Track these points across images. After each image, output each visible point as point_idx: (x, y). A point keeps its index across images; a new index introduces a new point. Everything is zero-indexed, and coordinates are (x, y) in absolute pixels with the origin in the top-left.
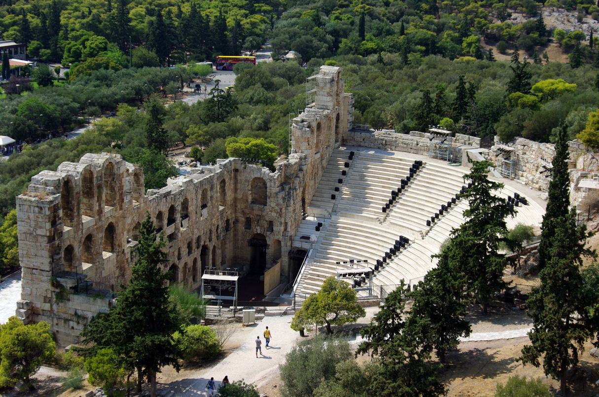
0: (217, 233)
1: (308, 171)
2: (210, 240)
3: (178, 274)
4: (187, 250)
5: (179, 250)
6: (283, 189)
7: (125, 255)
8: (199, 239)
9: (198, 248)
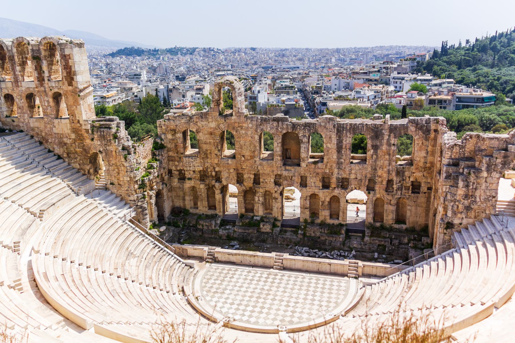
4: (321, 184)
6: (455, 164)
7: (81, 125)
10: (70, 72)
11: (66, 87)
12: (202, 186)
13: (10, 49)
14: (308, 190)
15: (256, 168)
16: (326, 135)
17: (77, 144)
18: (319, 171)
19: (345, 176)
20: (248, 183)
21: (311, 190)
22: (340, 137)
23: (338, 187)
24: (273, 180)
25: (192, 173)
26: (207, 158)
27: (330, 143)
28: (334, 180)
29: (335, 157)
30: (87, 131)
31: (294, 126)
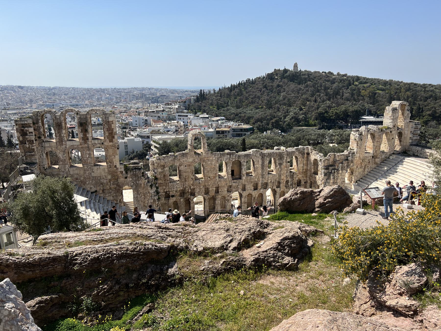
1: (355, 162)
2: (278, 187)
4: (253, 188)
7: (117, 169)
10: (112, 132)
11: (107, 143)
12: (182, 200)
13: (58, 117)
16: (256, 160)
17: (112, 182)
18: (252, 180)
19: (265, 181)
20: (212, 193)
22: (263, 160)
23: (262, 188)
24: (226, 189)
25: (174, 192)
26: (186, 181)
28: (260, 185)
30: (122, 172)
31: (239, 156)
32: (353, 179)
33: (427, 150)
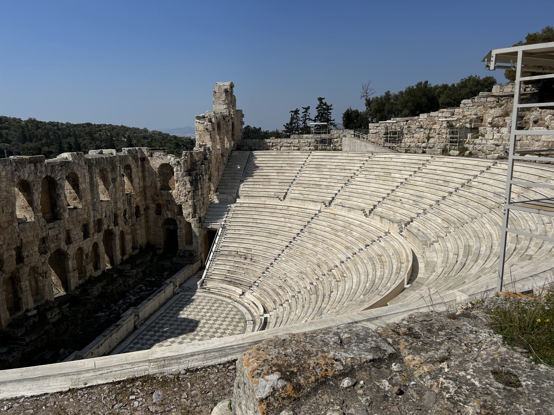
0: (125, 218)
1: (212, 161)
2: (116, 224)
3: (68, 262)
4: (82, 234)
5: (68, 232)
8: (99, 222)
9: (99, 231)
14: (74, 246)
15: (17, 238)
18: (81, 218)
19: (99, 217)
21: (76, 245)
23: (95, 232)
24: (37, 248)
27: (85, 183)
28: (91, 225)
29: (90, 198)
32: (213, 188)
33: (268, 141)
